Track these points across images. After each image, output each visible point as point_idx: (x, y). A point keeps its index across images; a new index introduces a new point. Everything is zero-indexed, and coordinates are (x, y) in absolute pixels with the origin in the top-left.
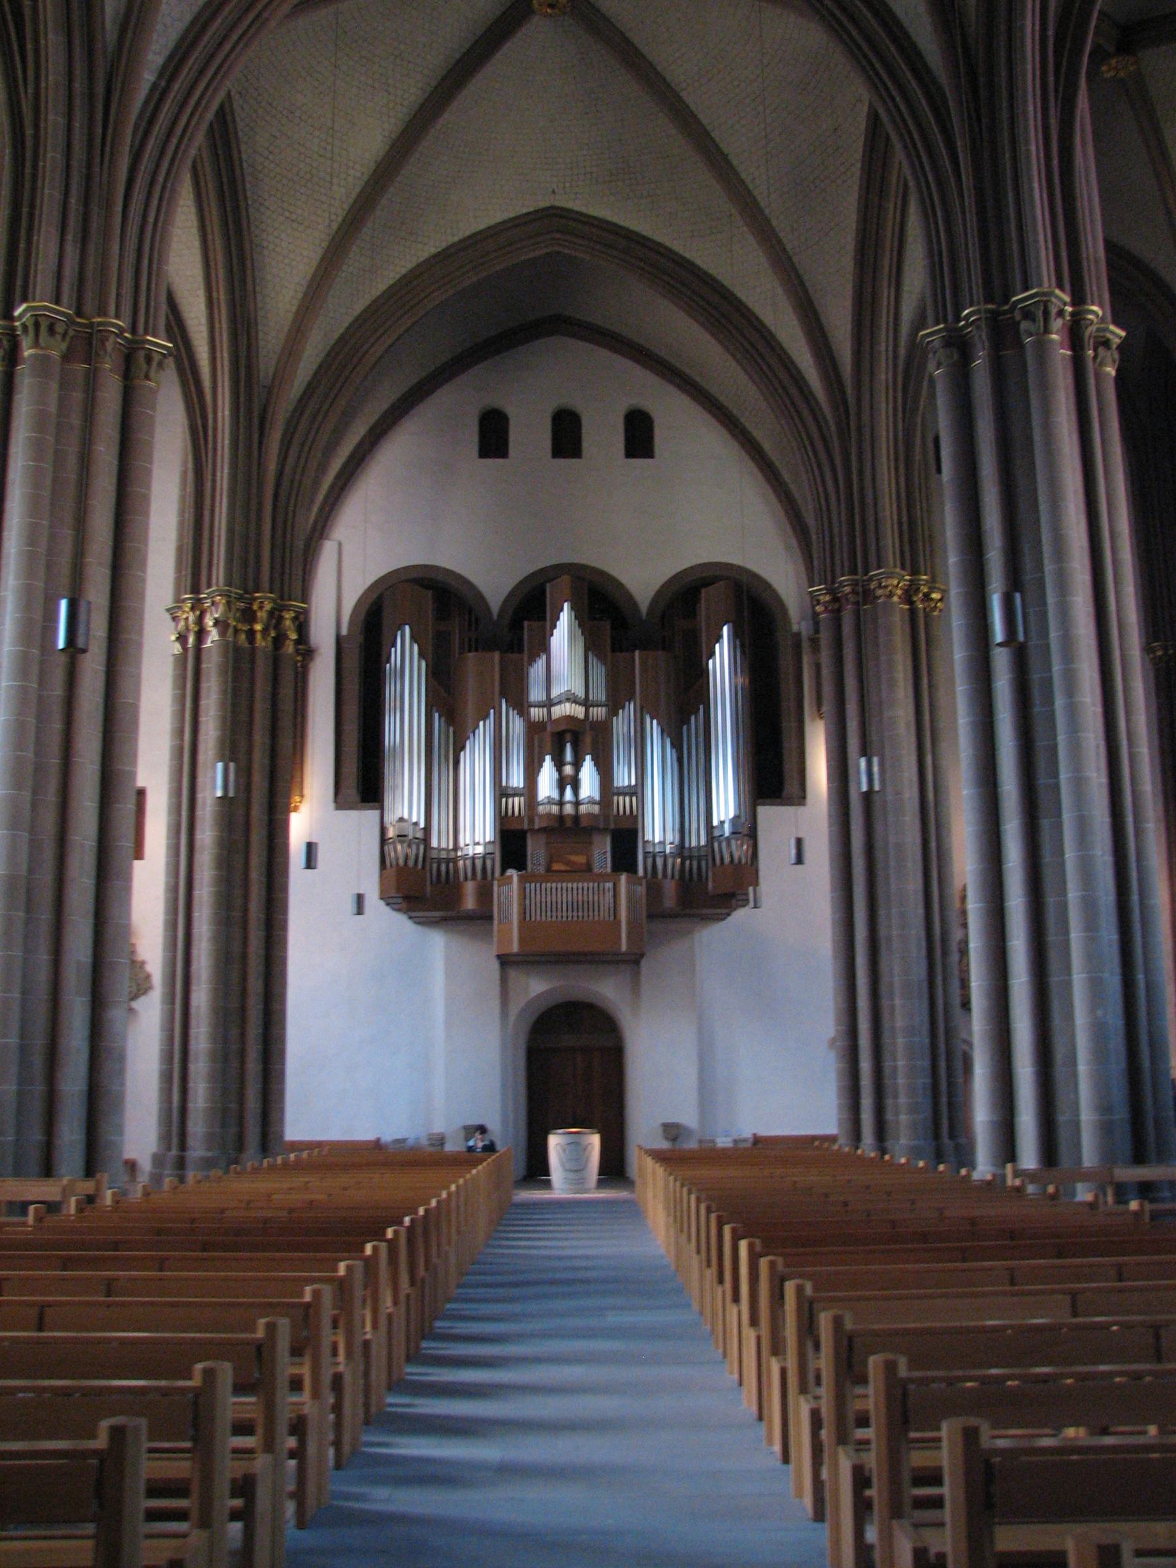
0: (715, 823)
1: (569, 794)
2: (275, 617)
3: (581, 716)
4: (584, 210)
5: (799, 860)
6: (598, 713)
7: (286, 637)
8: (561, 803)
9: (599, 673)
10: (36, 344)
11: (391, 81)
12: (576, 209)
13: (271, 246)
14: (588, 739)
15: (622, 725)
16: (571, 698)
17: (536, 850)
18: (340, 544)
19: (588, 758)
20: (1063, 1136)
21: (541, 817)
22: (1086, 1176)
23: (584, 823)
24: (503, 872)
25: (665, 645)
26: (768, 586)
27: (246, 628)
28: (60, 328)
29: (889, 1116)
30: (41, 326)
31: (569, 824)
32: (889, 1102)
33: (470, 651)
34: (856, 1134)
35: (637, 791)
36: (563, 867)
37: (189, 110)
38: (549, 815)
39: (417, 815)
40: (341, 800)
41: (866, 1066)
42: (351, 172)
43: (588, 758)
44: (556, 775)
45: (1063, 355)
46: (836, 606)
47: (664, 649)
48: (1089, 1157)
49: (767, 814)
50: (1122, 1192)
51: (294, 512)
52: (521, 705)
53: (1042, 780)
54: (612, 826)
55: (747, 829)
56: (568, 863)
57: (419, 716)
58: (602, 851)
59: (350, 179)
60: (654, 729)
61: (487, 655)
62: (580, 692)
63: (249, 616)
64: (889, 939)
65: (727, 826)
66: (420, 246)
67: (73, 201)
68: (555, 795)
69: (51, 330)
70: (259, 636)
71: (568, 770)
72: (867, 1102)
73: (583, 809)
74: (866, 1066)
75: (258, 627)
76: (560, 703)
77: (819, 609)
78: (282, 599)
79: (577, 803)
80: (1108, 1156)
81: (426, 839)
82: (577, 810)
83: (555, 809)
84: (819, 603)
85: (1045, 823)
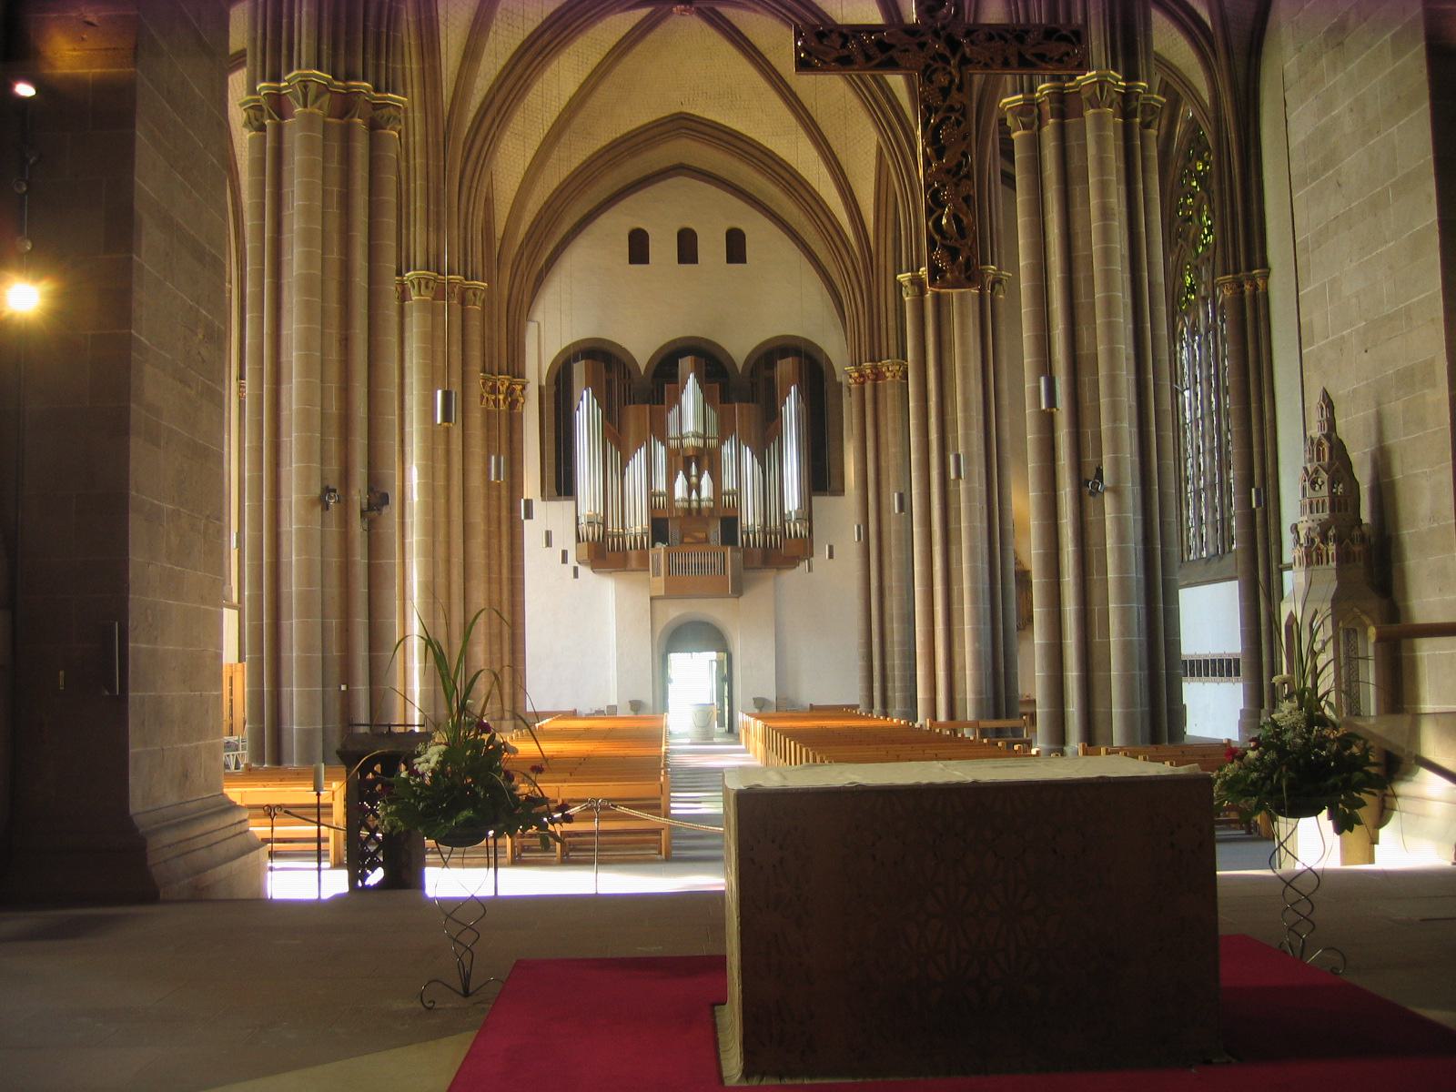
0: (786, 512)
1: (694, 492)
2: (510, 391)
3: (701, 445)
4: (701, 115)
5: (831, 556)
6: (713, 443)
7: (518, 401)
8: (689, 501)
9: (712, 415)
10: (420, 294)
11: (580, 51)
12: (697, 114)
13: (502, 151)
14: (706, 462)
15: (728, 450)
16: (696, 435)
17: (673, 530)
18: (539, 325)
19: (706, 472)
20: (958, 704)
21: (677, 509)
22: (968, 725)
23: (705, 513)
24: (653, 546)
25: (751, 398)
26: (820, 350)
27: (493, 397)
28: (431, 284)
29: (890, 693)
30: (423, 283)
31: (694, 513)
32: (890, 685)
33: (630, 404)
34: (871, 705)
35: (737, 493)
36: (691, 540)
37: (488, 142)
38: (683, 508)
39: (599, 510)
40: (545, 496)
41: (876, 663)
42: (553, 103)
43: (706, 472)
44: (686, 483)
45: (973, 294)
46: (862, 380)
47: (753, 402)
48: (970, 716)
49: (818, 501)
50: (984, 733)
51: (519, 320)
52: (664, 439)
53: (953, 525)
54: (721, 515)
55: (807, 514)
56: (695, 538)
57: (599, 451)
58: (715, 531)
59: (553, 108)
60: (747, 454)
61: (641, 406)
62: (701, 431)
63: (494, 390)
64: (891, 588)
65: (793, 513)
66: (596, 142)
67: (325, 47)
68: (687, 497)
69: (427, 287)
70: (501, 402)
71: (694, 480)
72: (877, 685)
73: (704, 504)
74: (876, 663)
75: (501, 397)
76: (688, 437)
77: (850, 381)
78: (514, 377)
79: (699, 500)
80: (980, 714)
81: (605, 527)
82: (699, 504)
83: (686, 505)
84: (851, 376)
85: (954, 548)
